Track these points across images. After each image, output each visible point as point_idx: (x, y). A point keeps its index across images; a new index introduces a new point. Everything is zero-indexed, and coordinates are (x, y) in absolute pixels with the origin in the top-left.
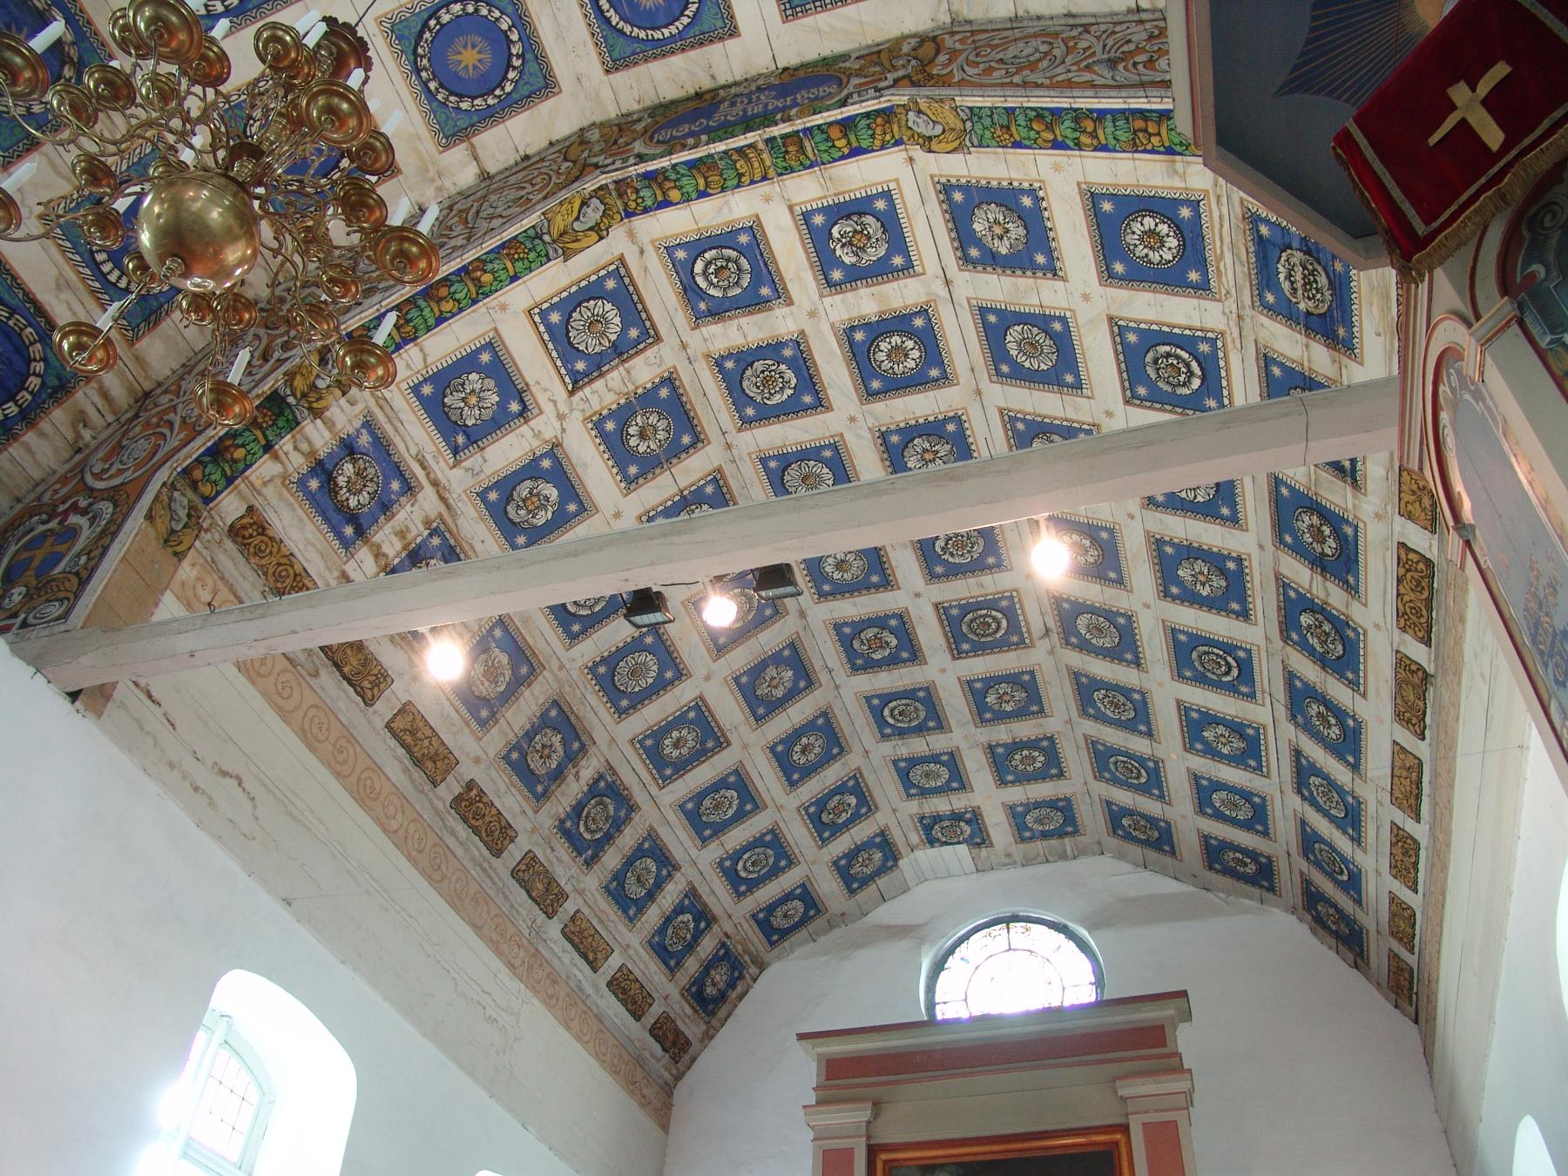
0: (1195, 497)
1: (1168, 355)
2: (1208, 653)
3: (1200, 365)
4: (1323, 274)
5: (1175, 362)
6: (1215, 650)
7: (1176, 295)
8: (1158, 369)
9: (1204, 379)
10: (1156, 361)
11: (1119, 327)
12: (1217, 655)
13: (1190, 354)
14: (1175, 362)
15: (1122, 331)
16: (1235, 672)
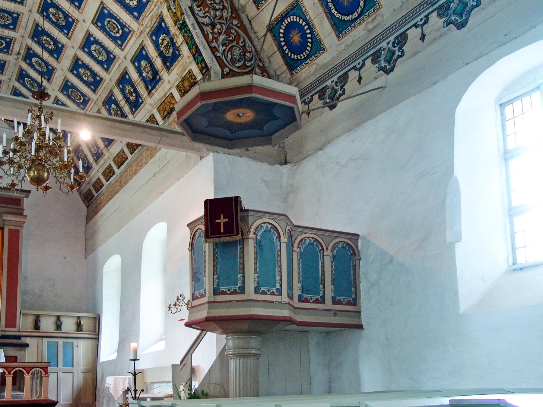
0: (98, 57)
1: (114, 23)
2: (76, 92)
3: (122, 32)
4: (172, 50)
5: (115, 26)
6: (78, 93)
7: (127, 13)
8: (108, 24)
9: (121, 36)
10: (109, 21)
11: (103, 6)
12: (78, 94)
13: (121, 28)
14: (115, 26)
15: (103, 8)
16: (81, 101)
